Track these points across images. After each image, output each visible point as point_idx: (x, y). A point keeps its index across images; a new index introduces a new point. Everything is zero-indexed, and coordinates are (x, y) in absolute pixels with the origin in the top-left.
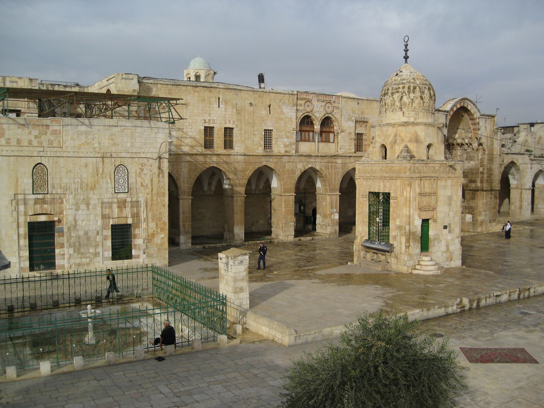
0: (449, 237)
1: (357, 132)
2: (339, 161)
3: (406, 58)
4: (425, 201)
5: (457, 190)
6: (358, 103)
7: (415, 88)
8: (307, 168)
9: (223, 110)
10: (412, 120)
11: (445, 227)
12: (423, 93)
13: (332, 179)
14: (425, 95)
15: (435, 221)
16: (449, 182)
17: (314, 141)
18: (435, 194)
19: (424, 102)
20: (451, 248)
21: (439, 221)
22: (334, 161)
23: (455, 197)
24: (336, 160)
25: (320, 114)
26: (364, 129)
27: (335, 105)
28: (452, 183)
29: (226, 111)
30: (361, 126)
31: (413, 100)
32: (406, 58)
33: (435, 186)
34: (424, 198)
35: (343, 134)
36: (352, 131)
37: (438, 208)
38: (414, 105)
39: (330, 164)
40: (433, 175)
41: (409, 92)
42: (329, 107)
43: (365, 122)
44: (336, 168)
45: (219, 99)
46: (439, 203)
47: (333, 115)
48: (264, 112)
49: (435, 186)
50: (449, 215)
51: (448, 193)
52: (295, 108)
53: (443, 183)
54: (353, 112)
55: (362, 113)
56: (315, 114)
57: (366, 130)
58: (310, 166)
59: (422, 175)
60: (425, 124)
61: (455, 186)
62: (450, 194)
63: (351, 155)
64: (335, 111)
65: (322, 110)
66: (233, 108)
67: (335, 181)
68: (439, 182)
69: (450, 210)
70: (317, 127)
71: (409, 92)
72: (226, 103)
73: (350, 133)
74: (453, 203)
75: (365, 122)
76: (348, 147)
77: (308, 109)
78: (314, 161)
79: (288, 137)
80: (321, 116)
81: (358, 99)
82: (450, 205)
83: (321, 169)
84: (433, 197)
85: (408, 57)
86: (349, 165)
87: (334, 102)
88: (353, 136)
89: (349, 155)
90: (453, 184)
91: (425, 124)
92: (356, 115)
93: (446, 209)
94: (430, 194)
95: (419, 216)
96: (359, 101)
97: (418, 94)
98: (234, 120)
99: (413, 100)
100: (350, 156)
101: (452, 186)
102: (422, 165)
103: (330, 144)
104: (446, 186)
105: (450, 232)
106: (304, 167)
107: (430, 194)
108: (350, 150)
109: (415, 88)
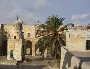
0: (18, 54)
3: (18, 19)
4: (11, 46)
11: (17, 52)
15: (14, 50)
16: (18, 43)
18: (14, 45)
20: (18, 56)
21: (15, 50)
23: (19, 46)
33: (14, 44)
48: (28, 29)
49: (14, 44)
51: (18, 45)
53: (16, 43)
68: (15, 43)
79: (33, 34)
105: (18, 53)
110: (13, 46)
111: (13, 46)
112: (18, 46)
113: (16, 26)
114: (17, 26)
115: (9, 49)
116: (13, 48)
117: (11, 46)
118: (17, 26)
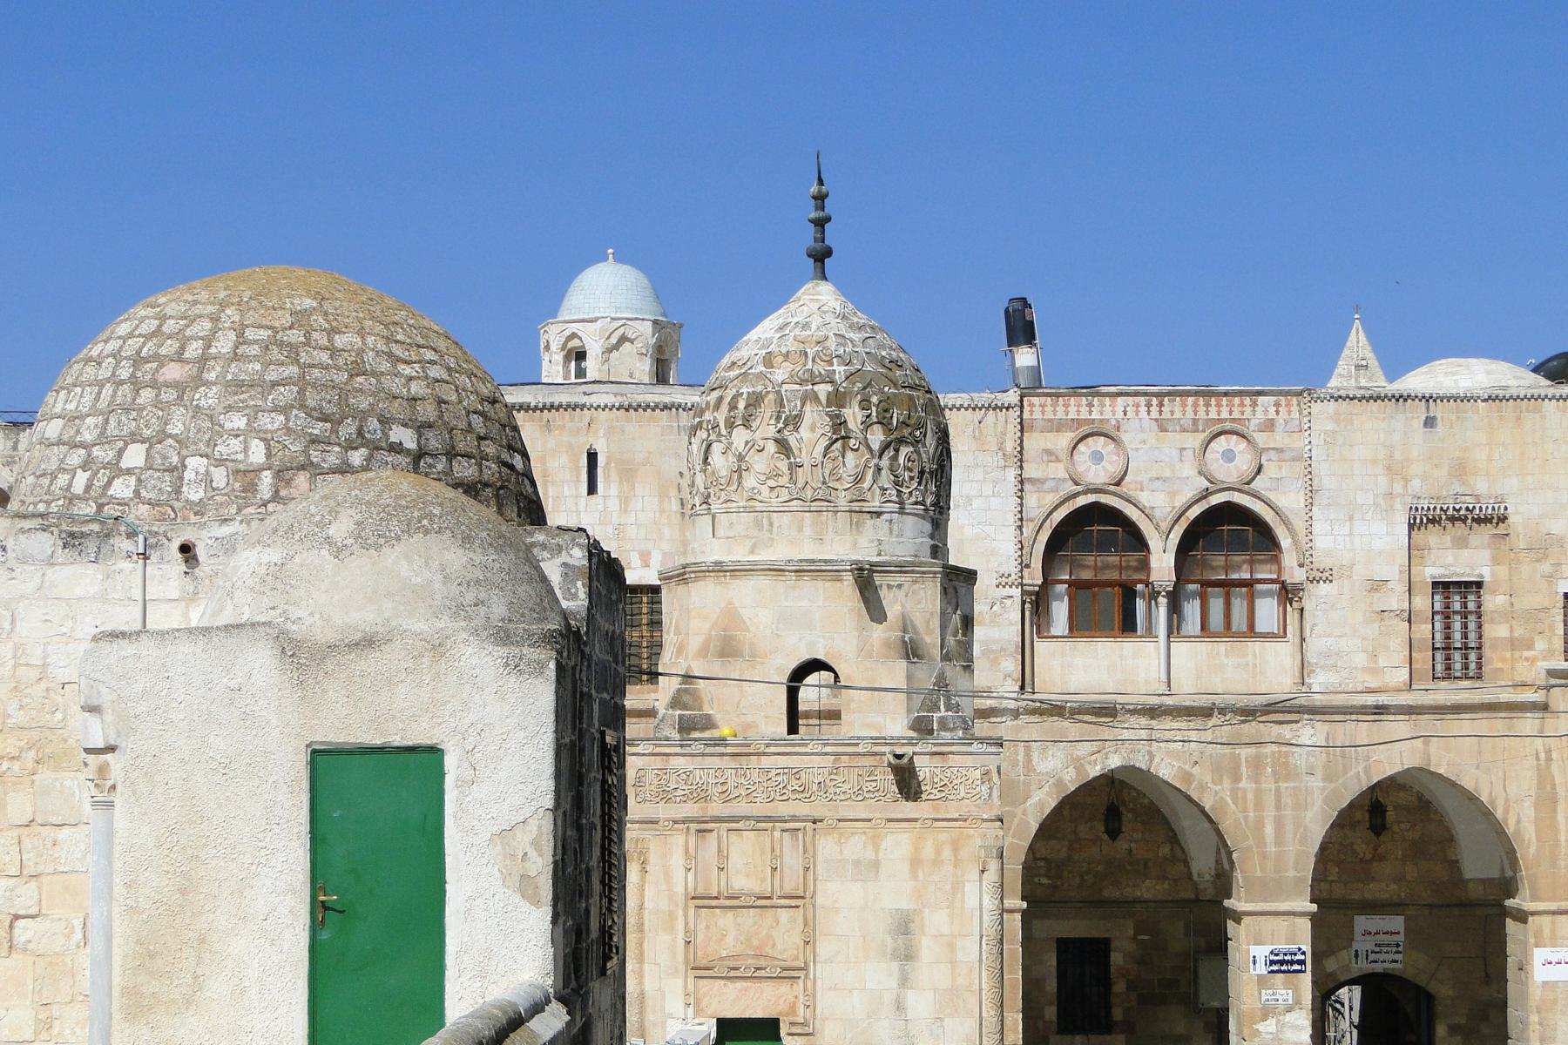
1: (1431, 571)
2: (1309, 733)
3: (821, 256)
4: (728, 933)
5: (958, 887)
6: (1430, 422)
7: (755, 401)
8: (1094, 771)
9: (614, 504)
10: (740, 554)
12: (795, 421)
13: (1259, 825)
14: (804, 432)
16: (897, 845)
17: (1150, 633)
19: (794, 467)
23: (936, 921)
24: (1286, 732)
25: (1173, 494)
26: (1486, 554)
27: (1279, 438)
28: (917, 850)
29: (624, 510)
30: (1461, 543)
31: (741, 458)
32: (821, 256)
33: (792, 860)
34: (726, 920)
35: (1323, 588)
36: (1393, 571)
37: (823, 973)
38: (750, 481)
39: (1245, 752)
40: (784, 809)
41: (731, 425)
42: (1229, 456)
43: (1487, 520)
44: (1284, 771)
45: (592, 457)
46: (824, 948)
47: (1255, 495)
49: (792, 860)
50: (900, 1007)
51: (894, 893)
52: (1012, 473)
53: (857, 846)
54: (1395, 470)
55: (1461, 470)
56: (1144, 498)
57: (1496, 561)
58: (1115, 762)
59: (716, 808)
60: (776, 570)
61: (937, 862)
62: (904, 904)
63: (1383, 699)
64: (1270, 470)
65: (1188, 470)
66: (663, 496)
67: (1279, 841)
69: (904, 981)
70: (1163, 563)
71: (731, 425)
72: (628, 472)
73: (1377, 585)
74: (927, 949)
75: (1487, 520)
76: (1361, 659)
77: (1097, 474)
78: (1144, 734)
80: (1181, 501)
81: (1427, 399)
82: (906, 955)
83: (1188, 777)
84: (784, 915)
85: (828, 253)
86: (1378, 753)
87: (1269, 426)
88: (1396, 599)
89: (1370, 700)
90: (928, 852)
91: (776, 570)
92: (1416, 484)
93: (881, 975)
94: (763, 902)
95: (695, 1003)
96: (1438, 410)
97: (766, 428)
98: (666, 547)
99: (741, 458)
100: (1380, 710)
101: (915, 862)
102: (716, 762)
103: (1254, 646)
104: (876, 865)
106: (1079, 769)
107: (763, 902)
108: (1374, 671)
109: (755, 401)
110: (783, 932)
111: (782, 934)
112: (904, 926)
113: (811, 435)
114: (853, 415)
115: (675, 1004)
116: (790, 973)
117: (728, 933)
118: (853, 415)
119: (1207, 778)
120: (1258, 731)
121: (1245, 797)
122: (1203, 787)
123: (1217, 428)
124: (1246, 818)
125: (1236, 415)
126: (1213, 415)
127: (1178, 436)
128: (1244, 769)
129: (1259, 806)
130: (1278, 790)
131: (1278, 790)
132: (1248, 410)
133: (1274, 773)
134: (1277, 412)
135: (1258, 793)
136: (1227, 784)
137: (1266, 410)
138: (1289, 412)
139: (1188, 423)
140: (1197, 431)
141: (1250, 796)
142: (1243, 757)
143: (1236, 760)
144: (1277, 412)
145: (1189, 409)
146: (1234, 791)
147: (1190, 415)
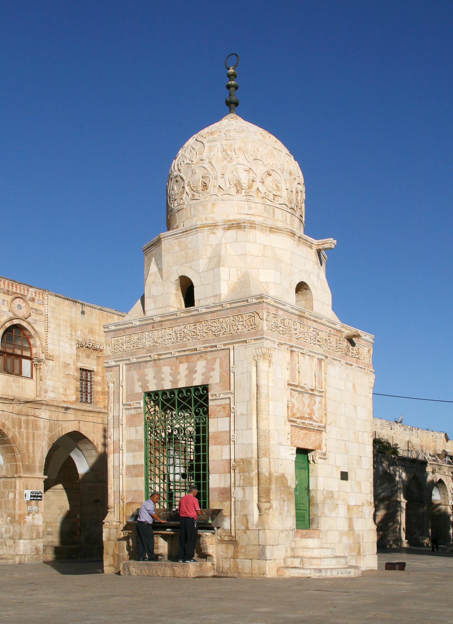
22: (31, 412)
39: (23, 418)
42: (20, 307)
119: (10, 426)
120: (27, 411)
121: (23, 435)
122: (8, 429)
123: (16, 296)
124: (23, 442)
125: (22, 293)
126: (14, 290)
127: (3, 295)
128: (23, 424)
129: (28, 439)
130: (34, 433)
131: (34, 433)
132: (26, 292)
133: (33, 427)
134: (36, 296)
135: (27, 433)
136: (17, 429)
137: (32, 294)
138: (39, 297)
139: (6, 291)
140: (8, 294)
141: (25, 435)
142: (22, 420)
143: (20, 420)
144: (36, 296)
145: (6, 286)
146: (19, 432)
147: (6, 288)
